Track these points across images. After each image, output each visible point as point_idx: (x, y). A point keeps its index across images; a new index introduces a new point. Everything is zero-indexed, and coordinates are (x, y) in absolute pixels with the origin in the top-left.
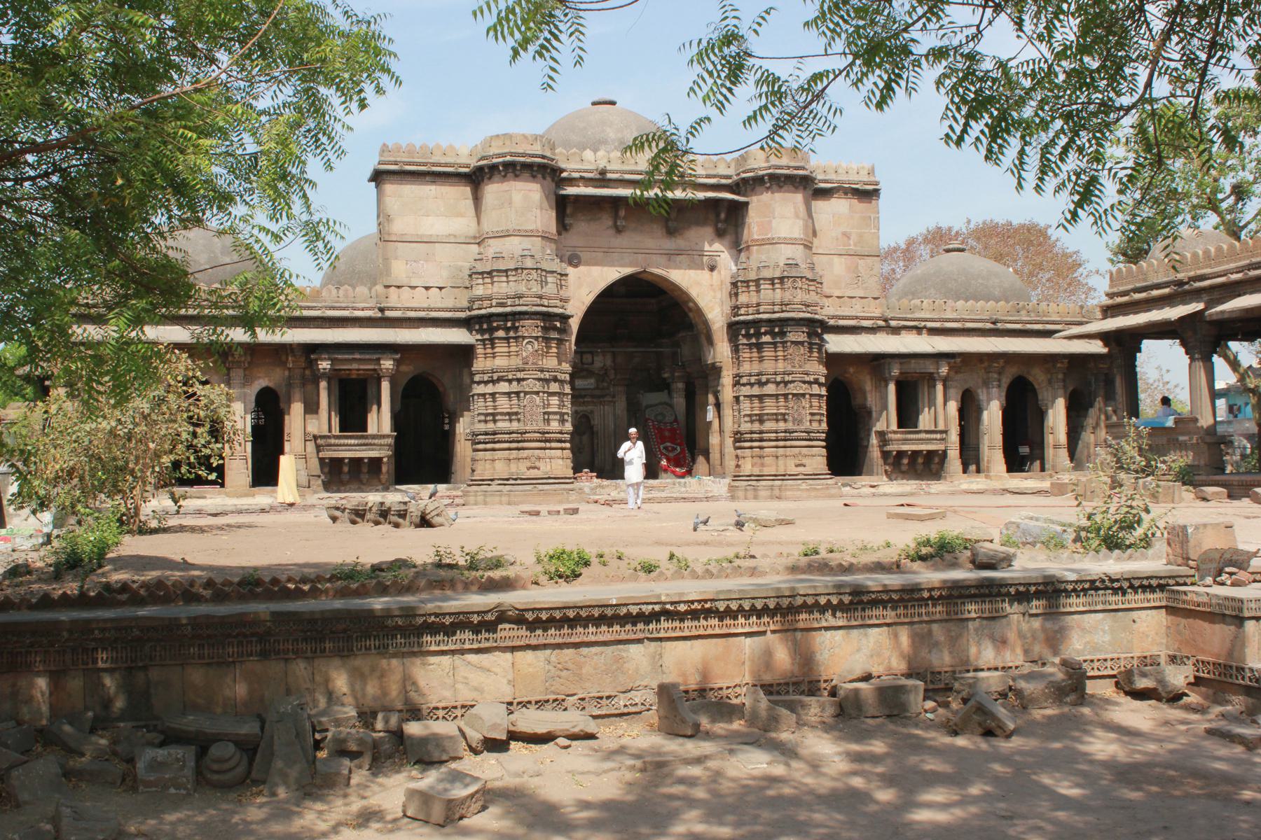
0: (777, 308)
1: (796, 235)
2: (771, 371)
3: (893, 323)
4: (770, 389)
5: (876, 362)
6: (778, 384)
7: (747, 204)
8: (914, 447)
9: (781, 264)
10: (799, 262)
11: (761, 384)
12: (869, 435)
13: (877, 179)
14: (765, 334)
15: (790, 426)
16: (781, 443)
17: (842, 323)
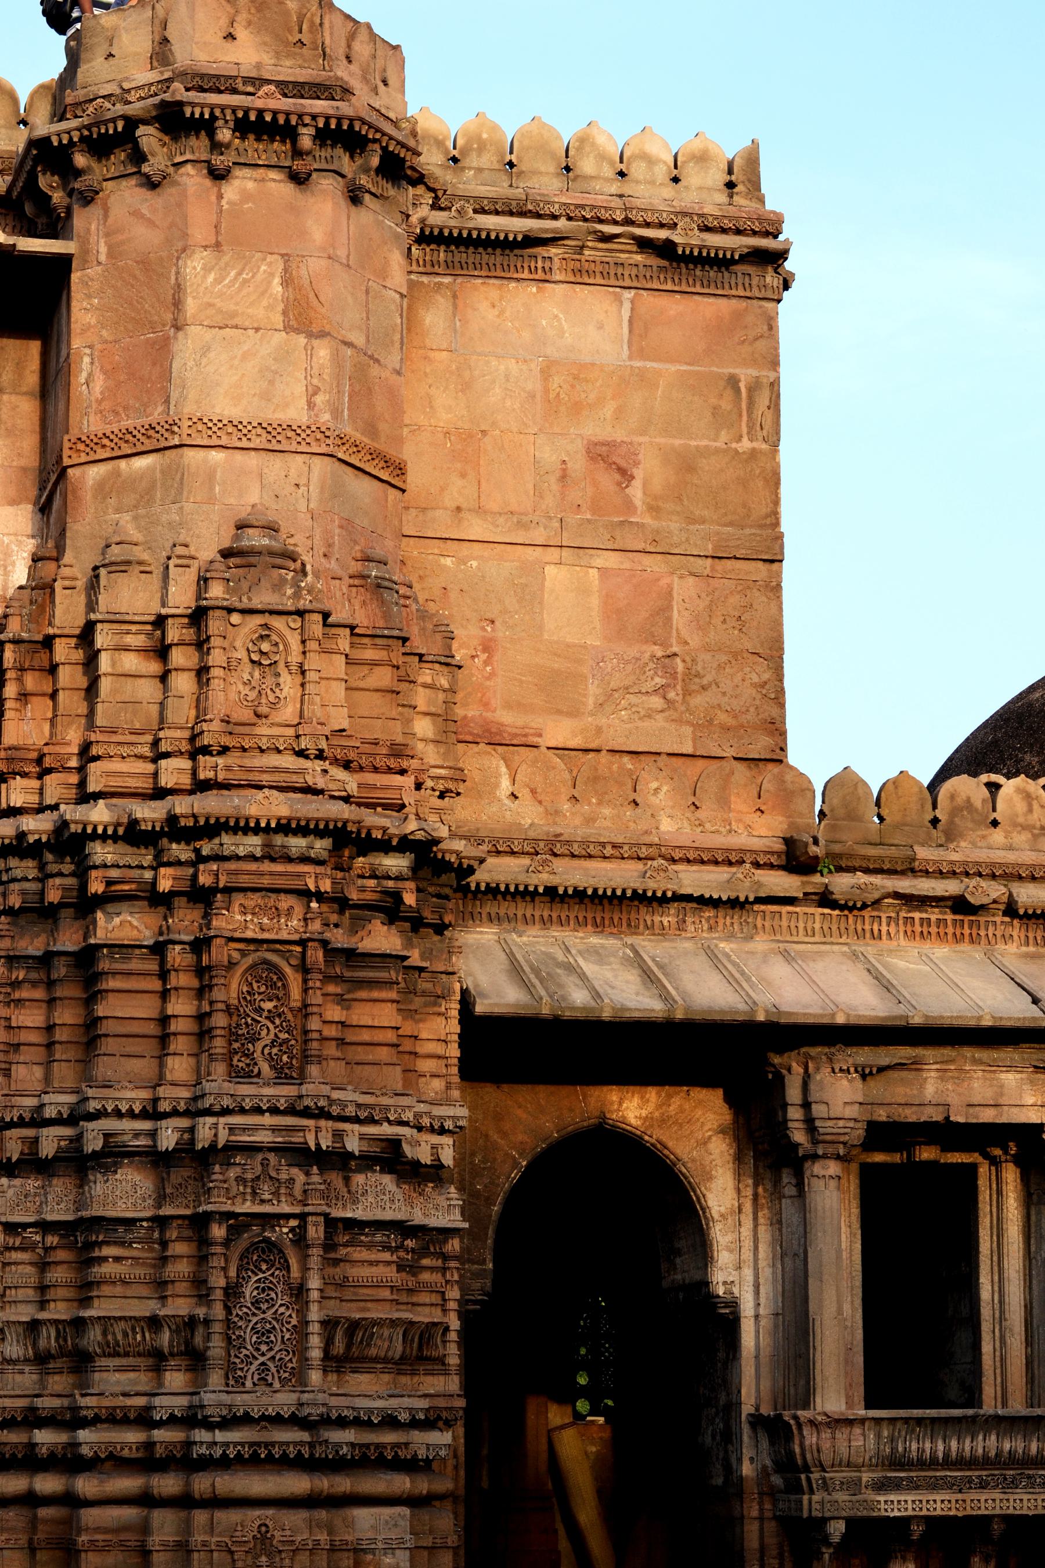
0: (174, 771)
1: (297, 413)
2: (136, 1097)
3: (842, 884)
4: (124, 1193)
5: (741, 1060)
6: (158, 1161)
7: (63, 264)
8: (939, 1503)
9: (207, 550)
10: (299, 544)
11: (79, 1164)
12: (729, 1437)
13: (769, 206)
14: (109, 899)
15: (215, 1396)
16: (168, 1484)
17: (570, 874)
